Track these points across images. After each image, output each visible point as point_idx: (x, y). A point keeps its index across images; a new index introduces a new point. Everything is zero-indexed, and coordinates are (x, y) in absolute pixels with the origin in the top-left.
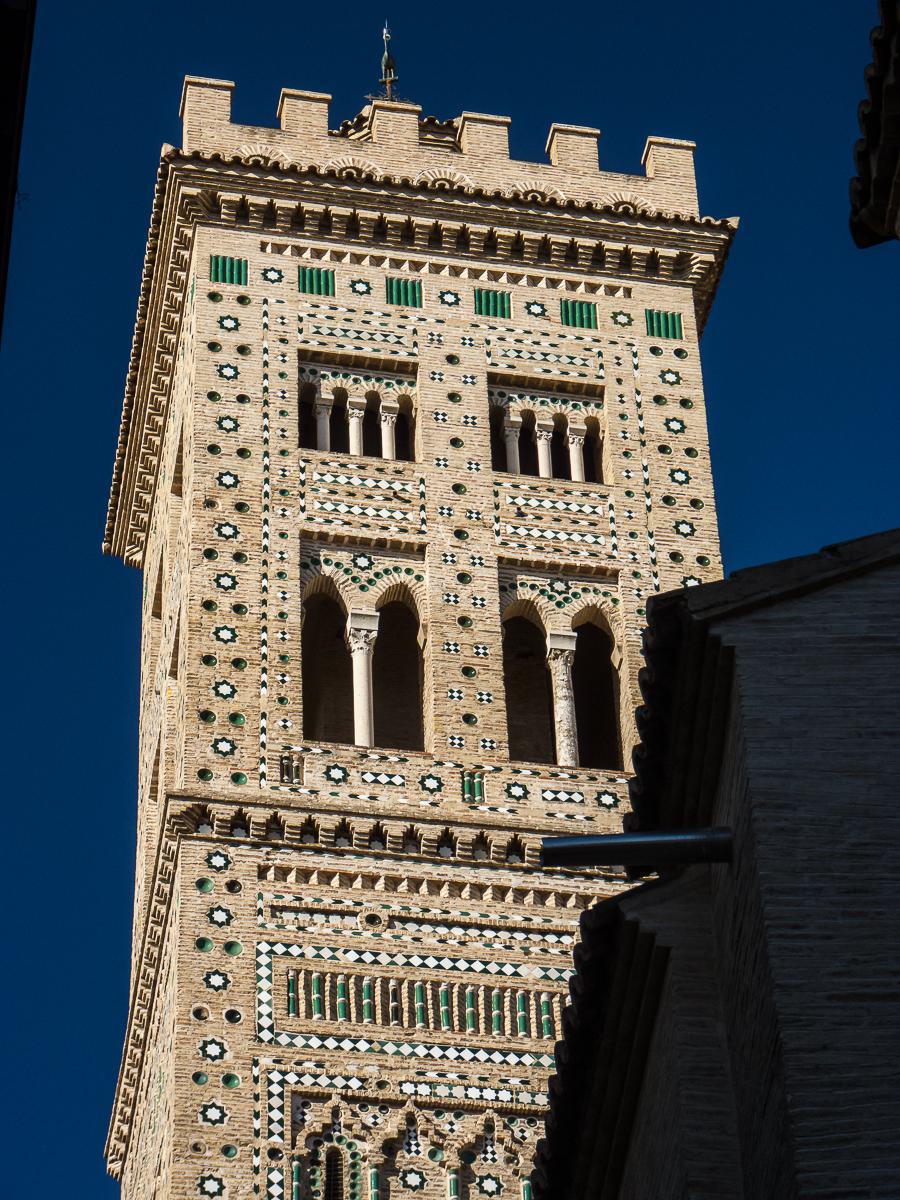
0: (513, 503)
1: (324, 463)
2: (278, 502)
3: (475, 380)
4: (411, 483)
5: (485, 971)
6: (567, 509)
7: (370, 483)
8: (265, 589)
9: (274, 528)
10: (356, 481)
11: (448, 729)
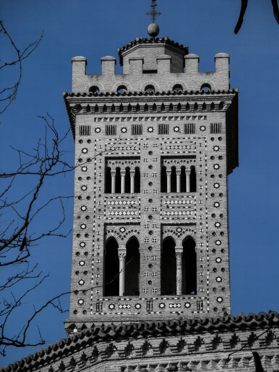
0: (166, 203)
1: (112, 198)
2: (98, 214)
3: (157, 160)
4: (137, 201)
6: (182, 203)
7: (125, 203)
8: (93, 246)
9: (96, 224)
10: (121, 203)
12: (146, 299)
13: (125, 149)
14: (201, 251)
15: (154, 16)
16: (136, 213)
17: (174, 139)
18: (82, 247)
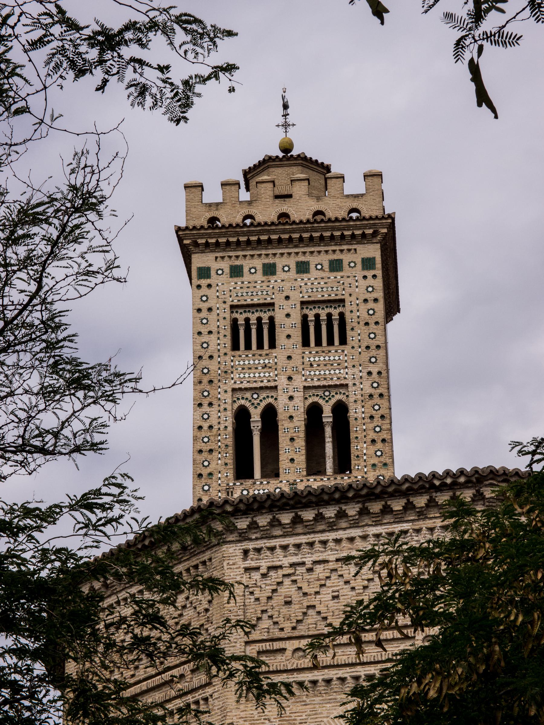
0: (309, 361)
7: (257, 362)
8: (219, 417)
10: (252, 362)
12: (288, 481)
13: (254, 294)
14: (356, 419)
15: (286, 128)
16: (271, 374)
17: (316, 279)
18: (206, 419)
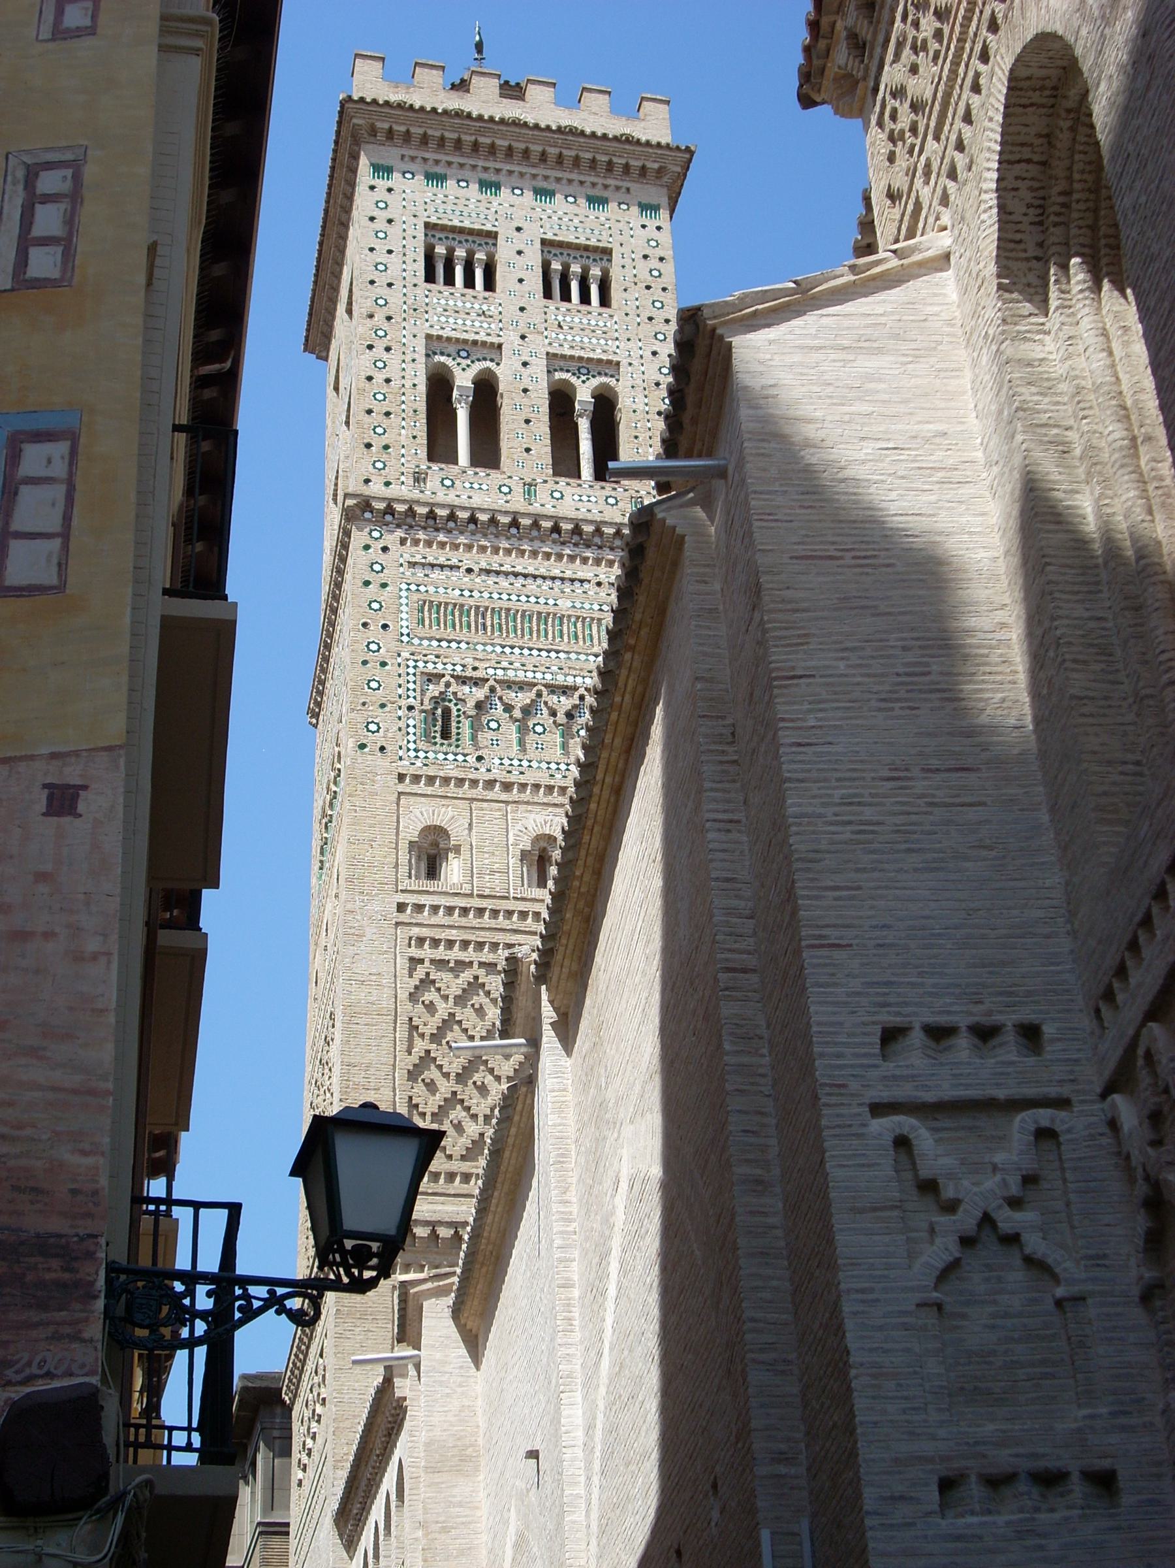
1: (440, 292)
5: (537, 603)
7: (468, 305)
10: (460, 304)
11: (515, 457)
